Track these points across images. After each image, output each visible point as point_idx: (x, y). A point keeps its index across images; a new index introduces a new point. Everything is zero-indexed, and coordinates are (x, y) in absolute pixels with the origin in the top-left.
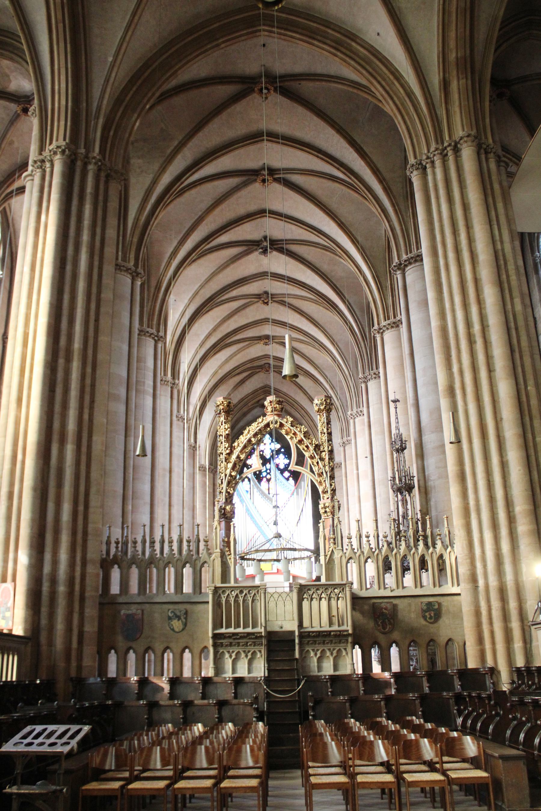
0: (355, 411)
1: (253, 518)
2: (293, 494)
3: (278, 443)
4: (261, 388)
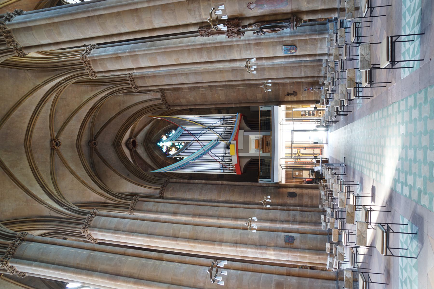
0: (88, 71)
1: (199, 156)
2: (183, 128)
3: (162, 137)
4: (115, 148)
